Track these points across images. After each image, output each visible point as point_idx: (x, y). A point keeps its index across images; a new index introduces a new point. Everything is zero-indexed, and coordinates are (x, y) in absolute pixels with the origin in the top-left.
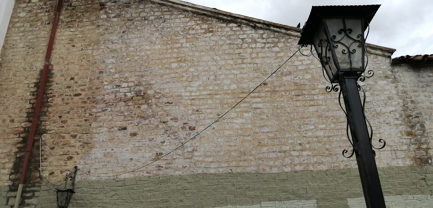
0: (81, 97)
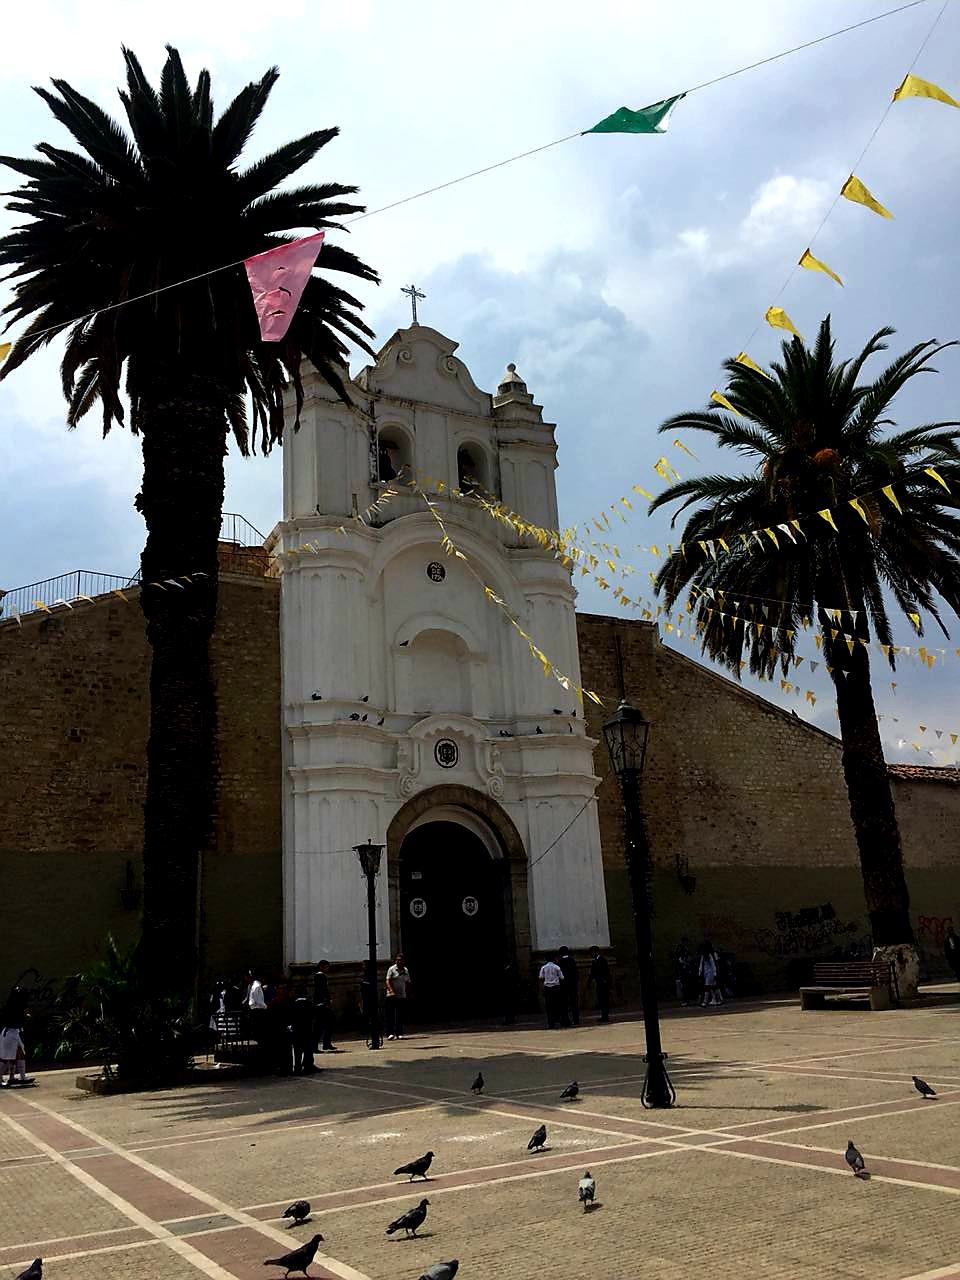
0: (665, 781)
